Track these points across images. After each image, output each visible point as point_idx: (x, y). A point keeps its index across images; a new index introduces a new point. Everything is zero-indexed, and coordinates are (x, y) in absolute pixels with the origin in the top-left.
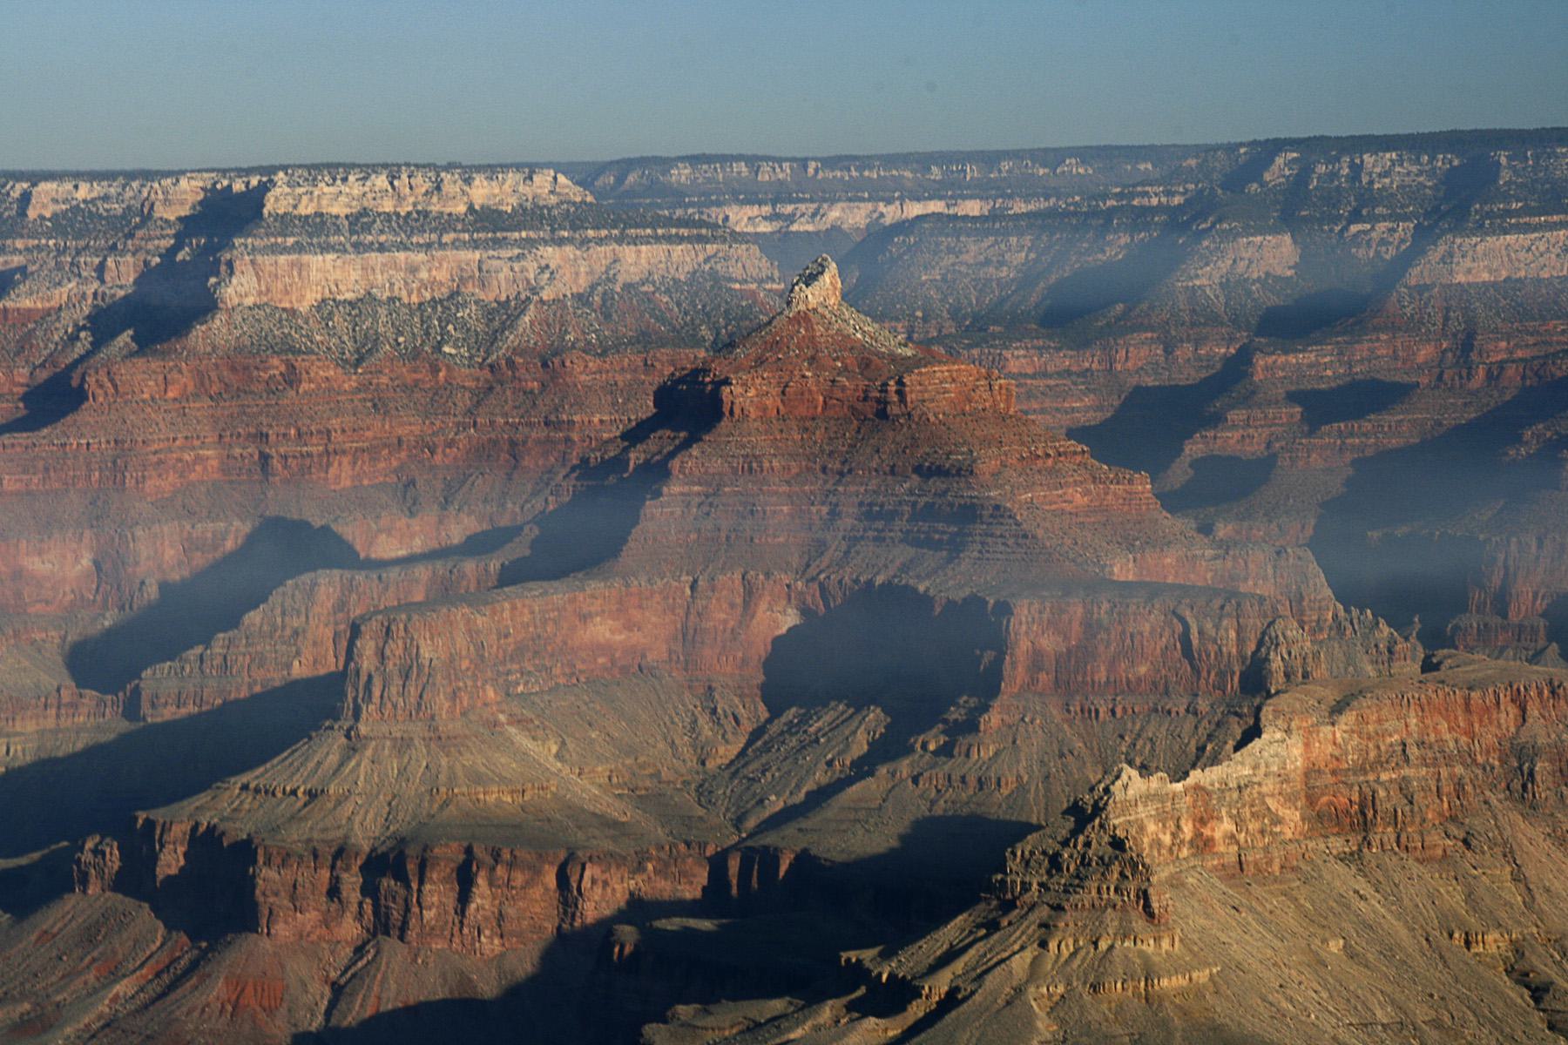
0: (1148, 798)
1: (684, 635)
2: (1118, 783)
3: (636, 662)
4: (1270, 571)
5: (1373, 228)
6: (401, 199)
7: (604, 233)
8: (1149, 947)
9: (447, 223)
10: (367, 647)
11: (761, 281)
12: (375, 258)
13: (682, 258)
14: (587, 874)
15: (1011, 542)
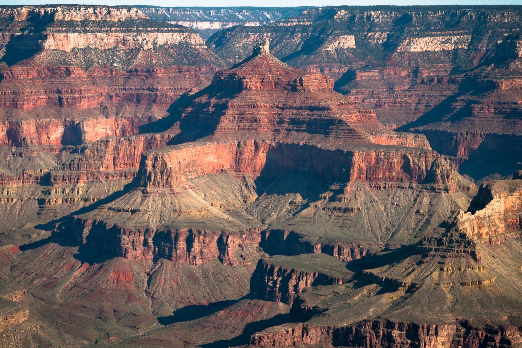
0: (468, 220)
1: (235, 160)
2: (459, 215)
3: (221, 168)
4: (414, 142)
5: (375, 34)
6: (97, 16)
7: (153, 29)
8: (477, 271)
9: (113, 24)
10: (149, 163)
11: (200, 45)
12: (90, 35)
13: (177, 38)
14: (230, 239)
15: (346, 132)
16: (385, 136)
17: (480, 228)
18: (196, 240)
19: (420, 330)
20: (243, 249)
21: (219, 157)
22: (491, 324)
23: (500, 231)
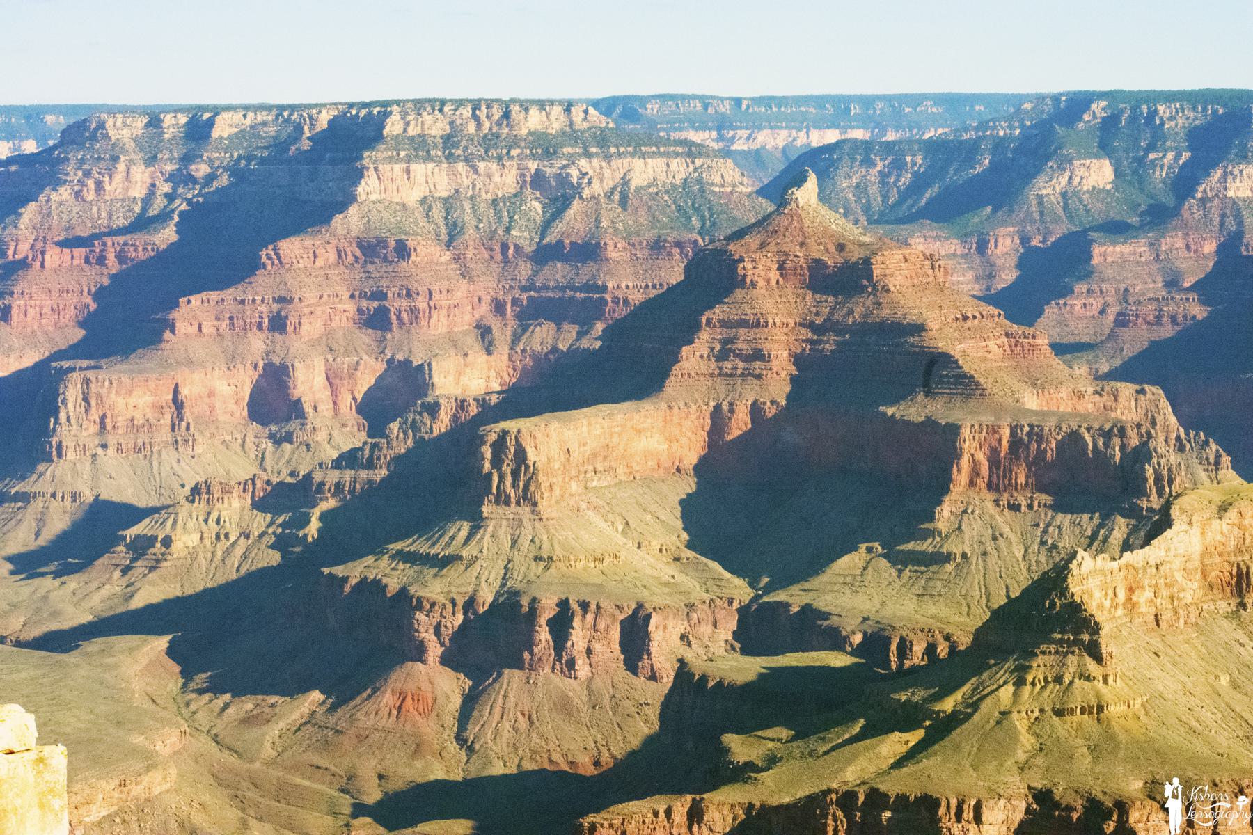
2: (1075, 562)
3: (677, 464)
4: (1133, 403)
5: (1164, 156)
6: (479, 125)
7: (622, 149)
9: (513, 143)
13: (679, 169)
16: (1064, 393)
17: (1131, 590)
18: (577, 622)
19: (942, 810)
20: (689, 644)
21: (670, 440)
22: (1100, 796)
23: (1188, 597)
